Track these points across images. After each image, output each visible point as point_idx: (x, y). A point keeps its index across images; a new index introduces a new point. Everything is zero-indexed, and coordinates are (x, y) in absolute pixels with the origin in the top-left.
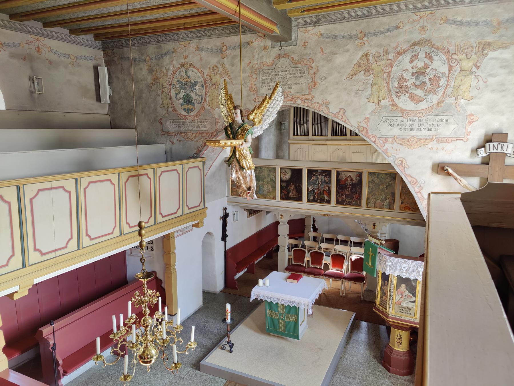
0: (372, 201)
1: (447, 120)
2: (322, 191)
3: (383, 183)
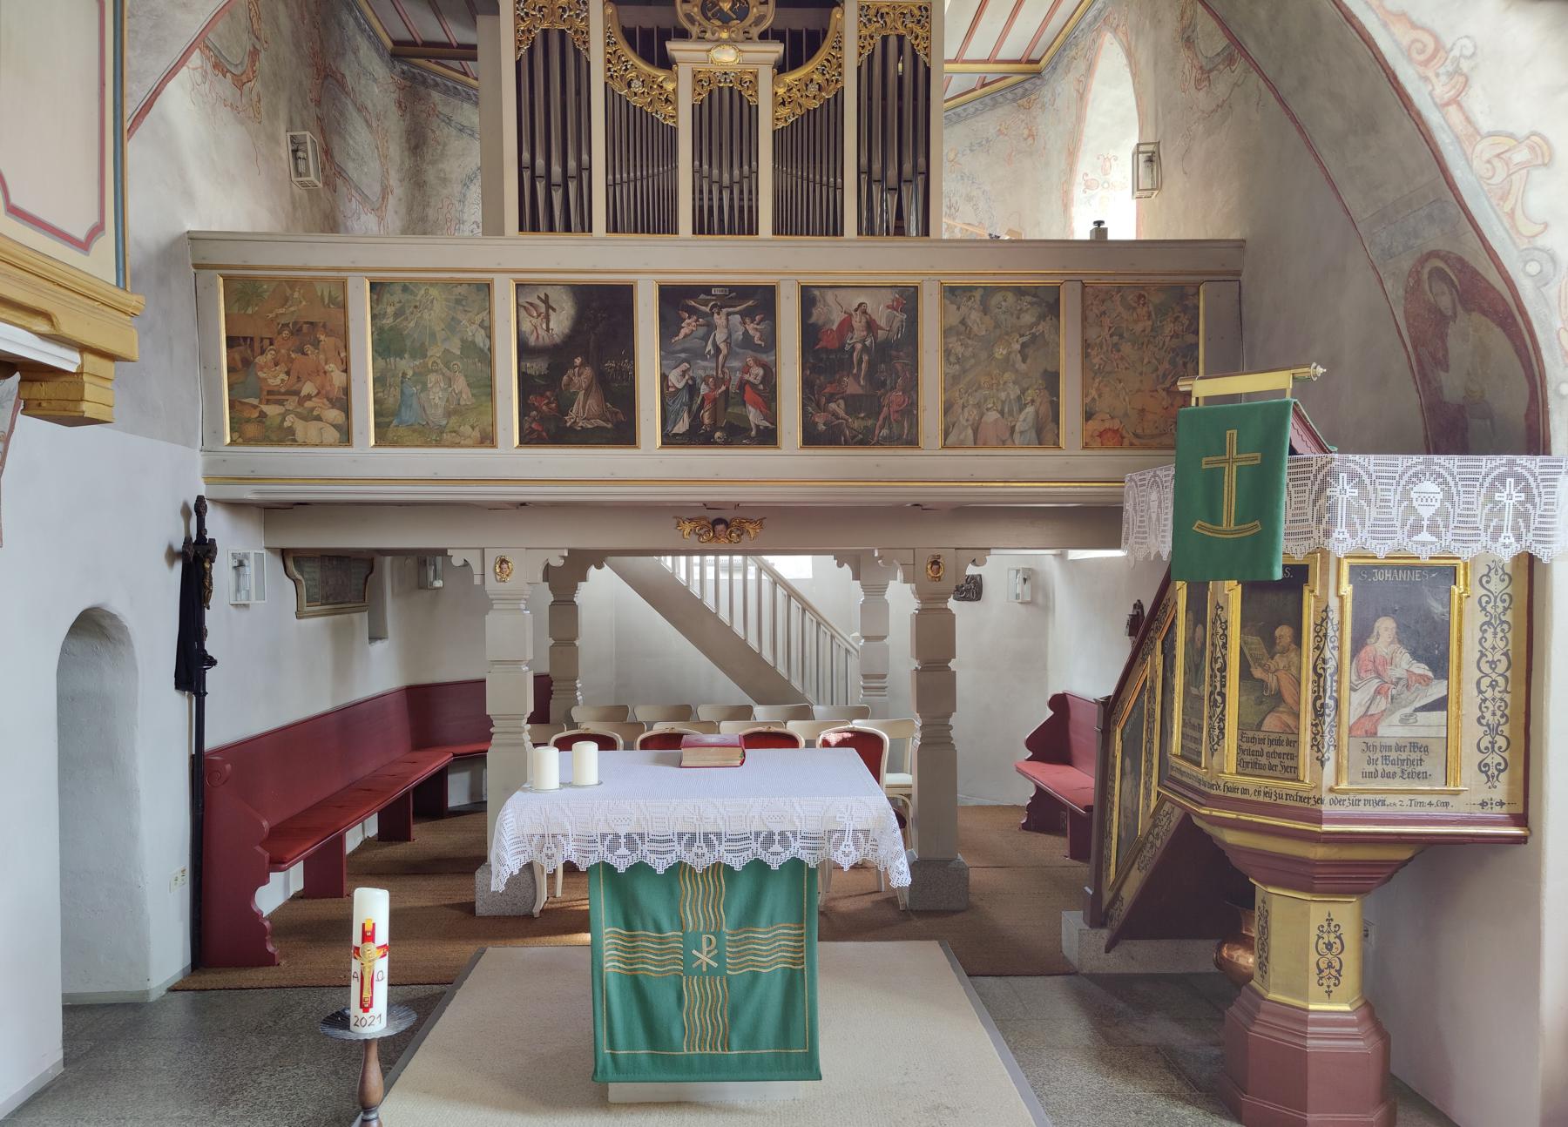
0: (966, 417)
2: (733, 389)
3: (1007, 334)
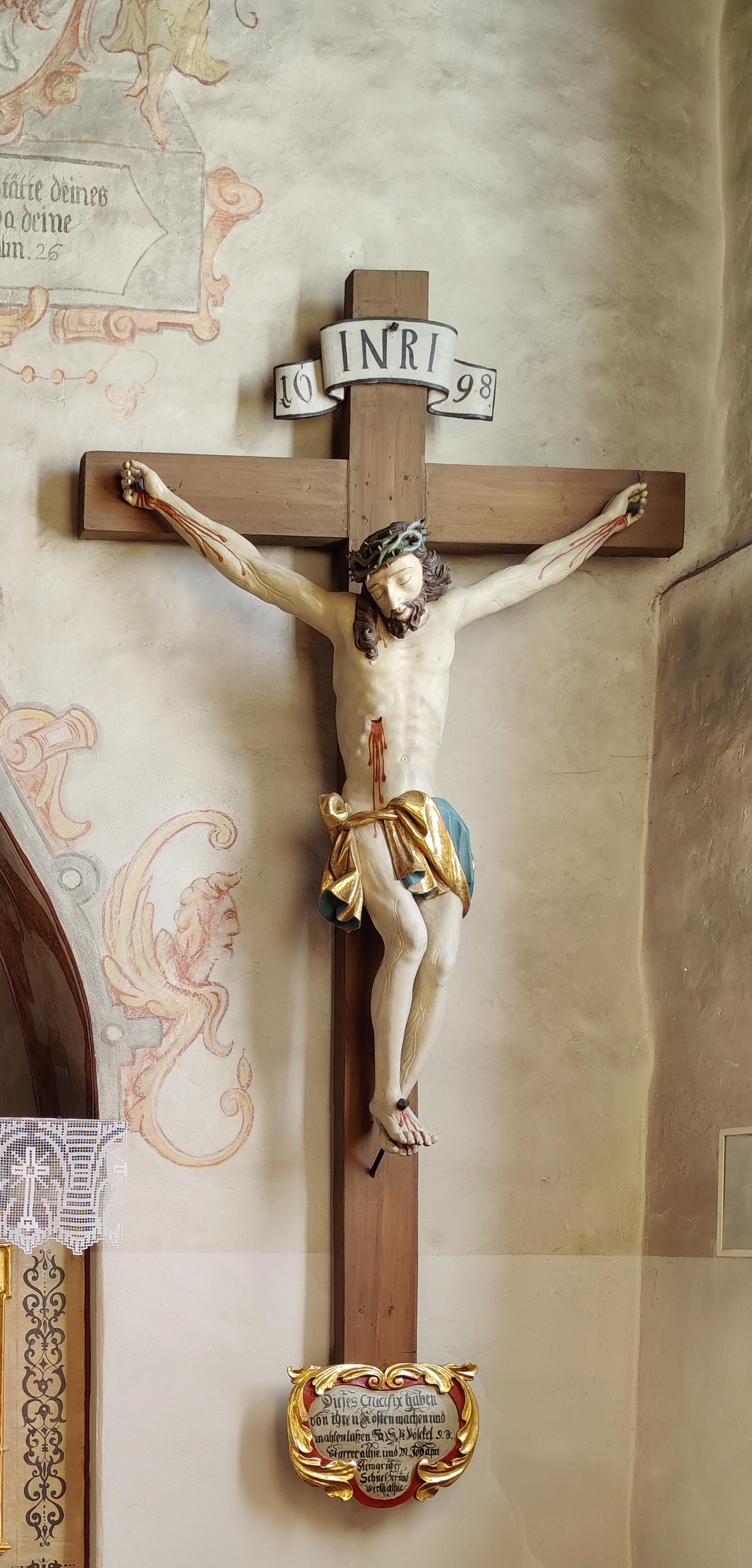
1: (102, 194)
